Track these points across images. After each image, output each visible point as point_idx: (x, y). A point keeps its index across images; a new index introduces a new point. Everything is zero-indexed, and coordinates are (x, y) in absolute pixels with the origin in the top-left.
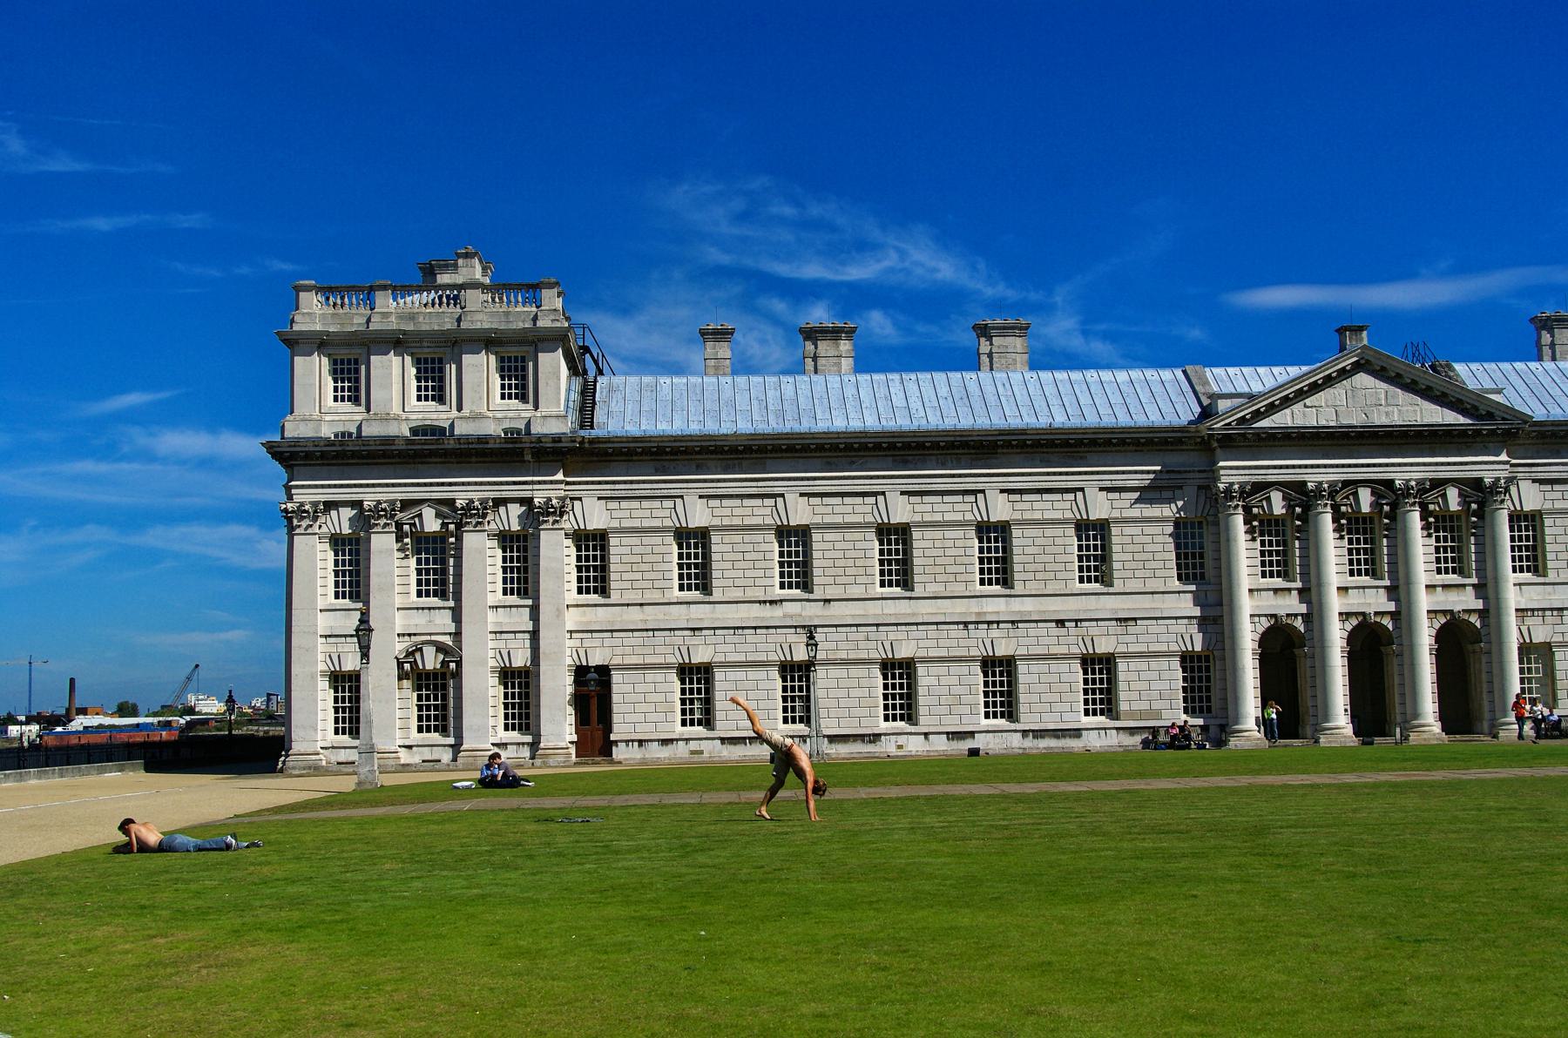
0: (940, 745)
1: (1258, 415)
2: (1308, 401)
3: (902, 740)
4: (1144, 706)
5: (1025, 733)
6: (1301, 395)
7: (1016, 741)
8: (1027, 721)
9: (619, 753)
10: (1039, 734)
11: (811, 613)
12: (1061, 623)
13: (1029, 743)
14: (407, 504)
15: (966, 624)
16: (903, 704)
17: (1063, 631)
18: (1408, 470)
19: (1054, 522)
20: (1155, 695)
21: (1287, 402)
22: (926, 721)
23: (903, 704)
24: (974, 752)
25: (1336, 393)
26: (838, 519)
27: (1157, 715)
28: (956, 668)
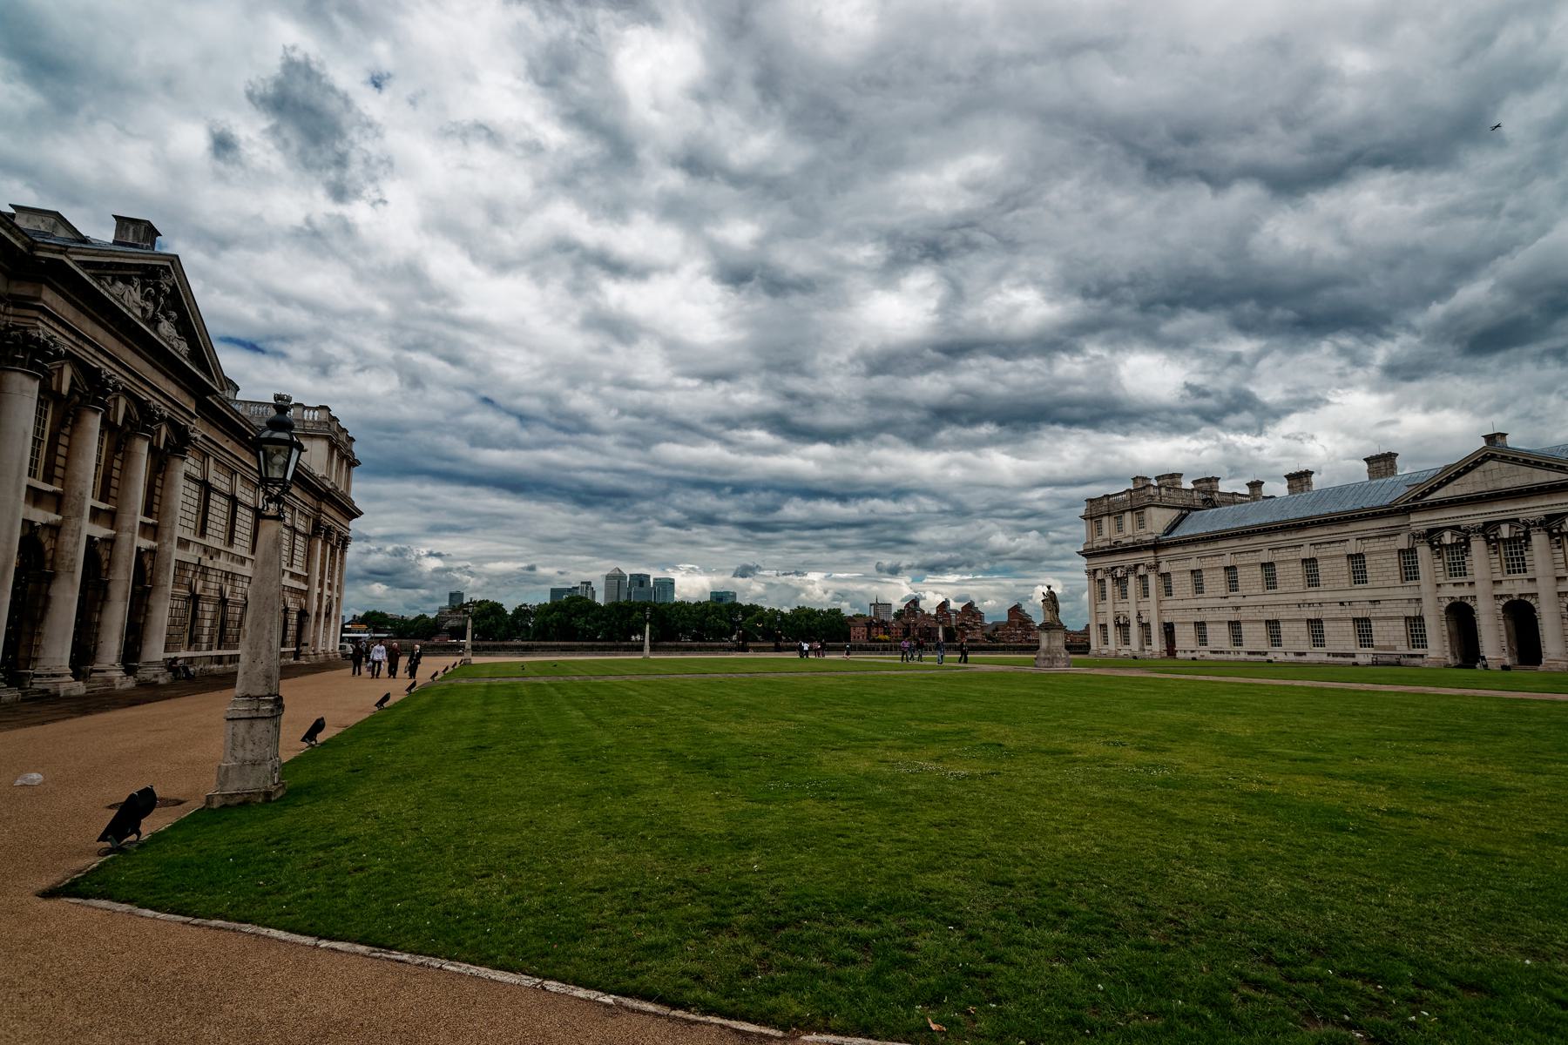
0: (1292, 657)
1: (1424, 494)
2: (1455, 482)
3: (1276, 655)
4: (1387, 644)
5: (1329, 654)
6: (1450, 480)
7: (1325, 658)
8: (1329, 648)
9: (1179, 655)
10: (1335, 655)
11: (1239, 601)
12: (1342, 604)
13: (1331, 659)
14: (1113, 568)
15: (1299, 605)
16: (1275, 639)
17: (1343, 607)
18: (1535, 509)
19: (1336, 556)
20: (1392, 638)
21: (1441, 485)
22: (1284, 647)
23: (1275, 639)
24: (1355, 664)
25: (1476, 475)
26: (1246, 562)
27: (1394, 648)
28: (1296, 625)
